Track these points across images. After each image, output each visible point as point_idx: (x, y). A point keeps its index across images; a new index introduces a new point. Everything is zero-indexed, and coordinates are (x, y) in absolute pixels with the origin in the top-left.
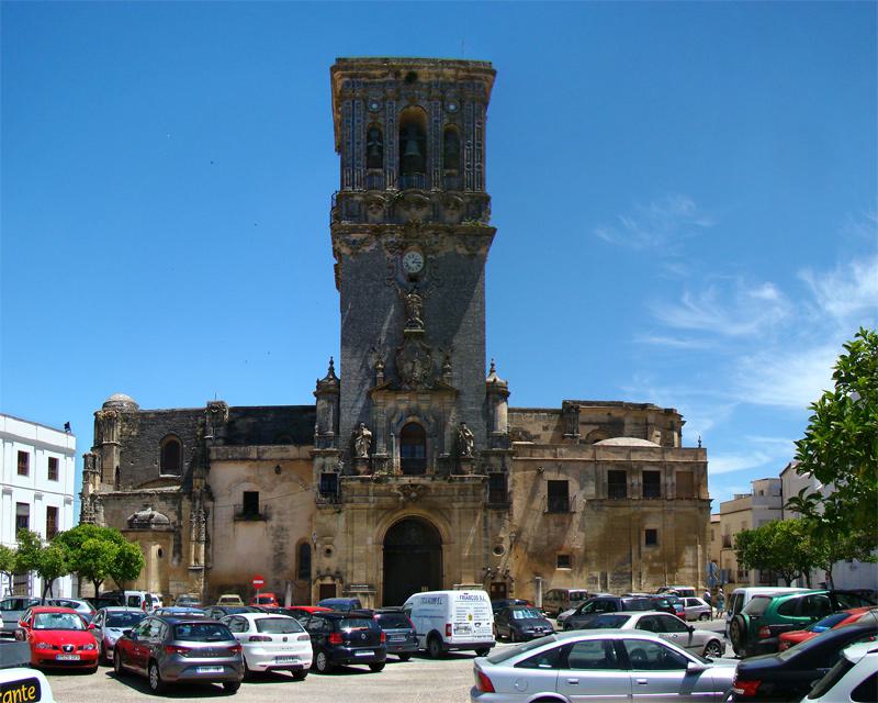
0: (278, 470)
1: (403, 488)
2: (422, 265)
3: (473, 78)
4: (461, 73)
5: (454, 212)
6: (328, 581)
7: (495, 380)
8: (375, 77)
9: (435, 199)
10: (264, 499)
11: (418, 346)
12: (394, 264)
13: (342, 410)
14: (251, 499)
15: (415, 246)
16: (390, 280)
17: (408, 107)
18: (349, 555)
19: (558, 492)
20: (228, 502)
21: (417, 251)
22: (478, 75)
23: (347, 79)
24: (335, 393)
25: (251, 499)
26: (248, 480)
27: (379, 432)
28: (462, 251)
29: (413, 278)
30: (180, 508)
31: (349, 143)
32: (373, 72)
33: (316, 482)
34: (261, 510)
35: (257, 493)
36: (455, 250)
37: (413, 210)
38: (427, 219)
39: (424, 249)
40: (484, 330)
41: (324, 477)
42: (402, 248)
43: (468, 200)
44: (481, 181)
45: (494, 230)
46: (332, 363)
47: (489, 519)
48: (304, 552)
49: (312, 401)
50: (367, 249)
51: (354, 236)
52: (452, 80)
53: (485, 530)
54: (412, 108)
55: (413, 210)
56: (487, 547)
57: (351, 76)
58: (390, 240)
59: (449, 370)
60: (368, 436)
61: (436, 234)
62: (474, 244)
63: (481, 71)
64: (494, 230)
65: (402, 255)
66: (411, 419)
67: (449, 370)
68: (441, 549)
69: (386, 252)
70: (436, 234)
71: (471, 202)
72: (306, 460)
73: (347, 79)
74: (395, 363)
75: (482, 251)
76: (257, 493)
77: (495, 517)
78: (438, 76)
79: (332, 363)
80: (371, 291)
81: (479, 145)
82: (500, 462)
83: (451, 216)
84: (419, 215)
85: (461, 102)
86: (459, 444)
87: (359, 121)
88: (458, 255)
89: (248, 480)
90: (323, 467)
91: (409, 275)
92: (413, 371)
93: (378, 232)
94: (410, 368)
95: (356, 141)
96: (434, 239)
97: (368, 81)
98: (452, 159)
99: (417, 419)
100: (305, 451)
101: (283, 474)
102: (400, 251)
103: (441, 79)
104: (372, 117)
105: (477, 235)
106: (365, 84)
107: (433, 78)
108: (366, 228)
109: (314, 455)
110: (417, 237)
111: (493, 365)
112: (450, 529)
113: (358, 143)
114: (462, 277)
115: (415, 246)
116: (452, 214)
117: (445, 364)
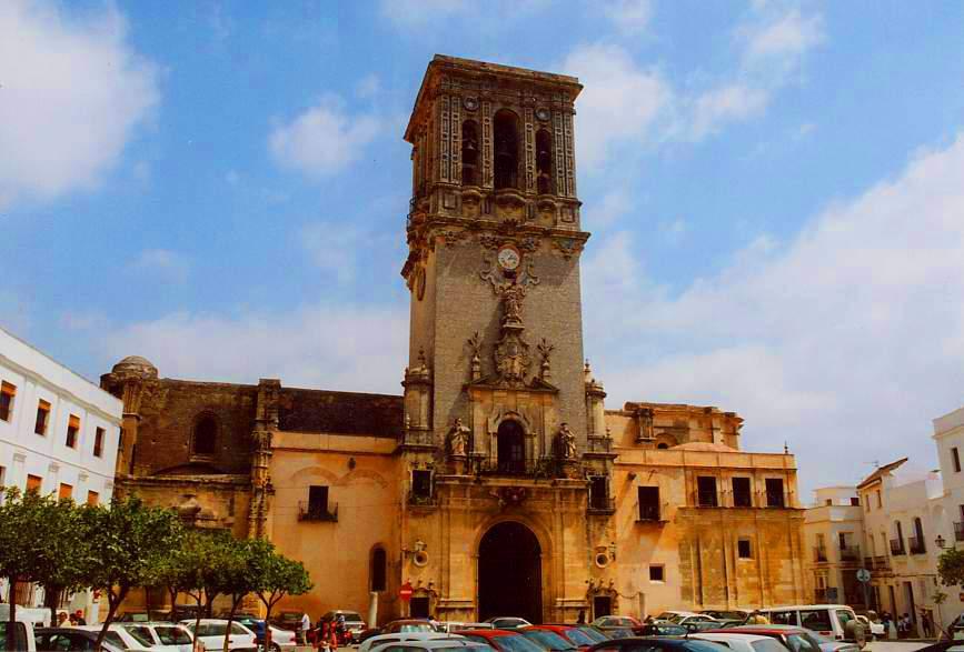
0: (352, 465)
1: (503, 490)
2: (518, 262)
5: (548, 215)
6: (421, 595)
7: (593, 381)
10: (334, 496)
11: (516, 341)
12: (490, 259)
13: (436, 403)
14: (318, 495)
17: (501, 110)
18: (445, 563)
19: (649, 498)
20: (292, 497)
24: (428, 384)
25: (318, 495)
26: (317, 472)
27: (475, 429)
30: (232, 502)
31: (445, 136)
33: (407, 484)
34: (331, 510)
35: (326, 488)
38: (524, 219)
40: (581, 330)
41: (417, 474)
42: (499, 245)
44: (573, 187)
45: (584, 237)
46: (421, 353)
47: (592, 527)
48: (379, 558)
49: (399, 391)
50: (463, 242)
51: (450, 229)
53: (588, 539)
56: (590, 558)
57: (448, 72)
59: (548, 368)
60: (465, 433)
63: (569, 84)
64: (584, 237)
65: (498, 251)
66: (508, 417)
67: (548, 368)
68: (540, 559)
71: (564, 207)
72: (386, 455)
74: (493, 358)
75: (577, 254)
76: (326, 488)
77: (597, 525)
79: (421, 353)
81: (569, 152)
82: (601, 466)
85: (551, 110)
86: (560, 443)
89: (317, 472)
90: (415, 464)
92: (512, 367)
94: (509, 366)
95: (453, 134)
98: (545, 162)
99: (515, 417)
100: (385, 444)
101: (356, 469)
104: (468, 115)
109: (399, 452)
110: (514, 235)
111: (587, 365)
112: (551, 537)
116: (546, 217)
117: (543, 362)
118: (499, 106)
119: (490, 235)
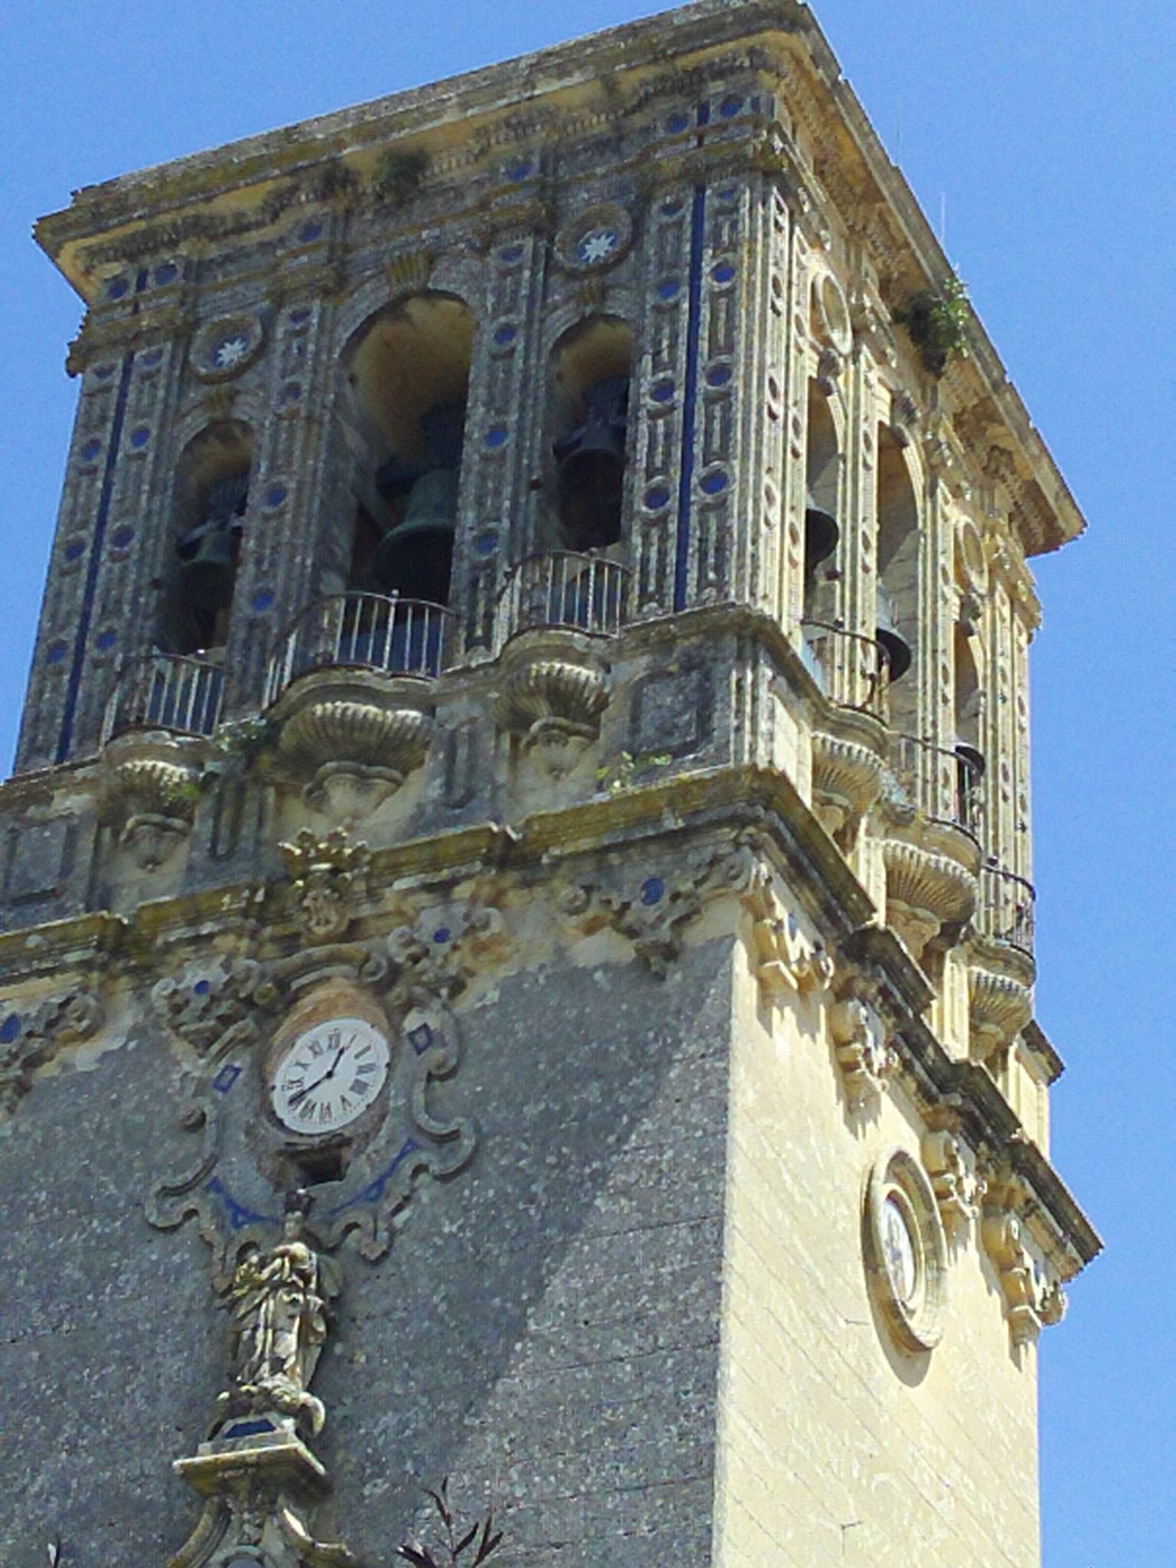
2: (376, 1080)
3: (692, 82)
4: (632, 79)
8: (242, 227)
9: (459, 710)
15: (339, 984)
16: (180, 1191)
17: (394, 308)
21: (352, 1009)
22: (714, 53)
23: (115, 269)
28: (600, 949)
29: (322, 1161)
32: (225, 205)
36: (560, 952)
37: (341, 796)
39: (387, 988)
42: (265, 1011)
43: (639, 666)
50: (84, 1056)
52: (599, 125)
54: (416, 308)
55: (341, 796)
57: (129, 251)
58: (193, 977)
61: (443, 889)
62: (652, 890)
69: (179, 1047)
70: (443, 889)
71: (656, 675)
73: (115, 269)
78: (518, 126)
80: (71, 1270)
83: (556, 788)
84: (371, 816)
87: (141, 436)
88: (575, 979)
91: (291, 1153)
93: (127, 952)
95: (113, 526)
96: (431, 919)
97: (214, 251)
98: (587, 493)
102: (248, 1025)
103: (539, 137)
105: (674, 839)
106: (198, 270)
107: (505, 148)
108: (66, 940)
110: (353, 930)
113: (123, 537)
114: (594, 1092)
115: (339, 984)
116: (556, 771)
118: (367, 299)
119: (215, 974)
